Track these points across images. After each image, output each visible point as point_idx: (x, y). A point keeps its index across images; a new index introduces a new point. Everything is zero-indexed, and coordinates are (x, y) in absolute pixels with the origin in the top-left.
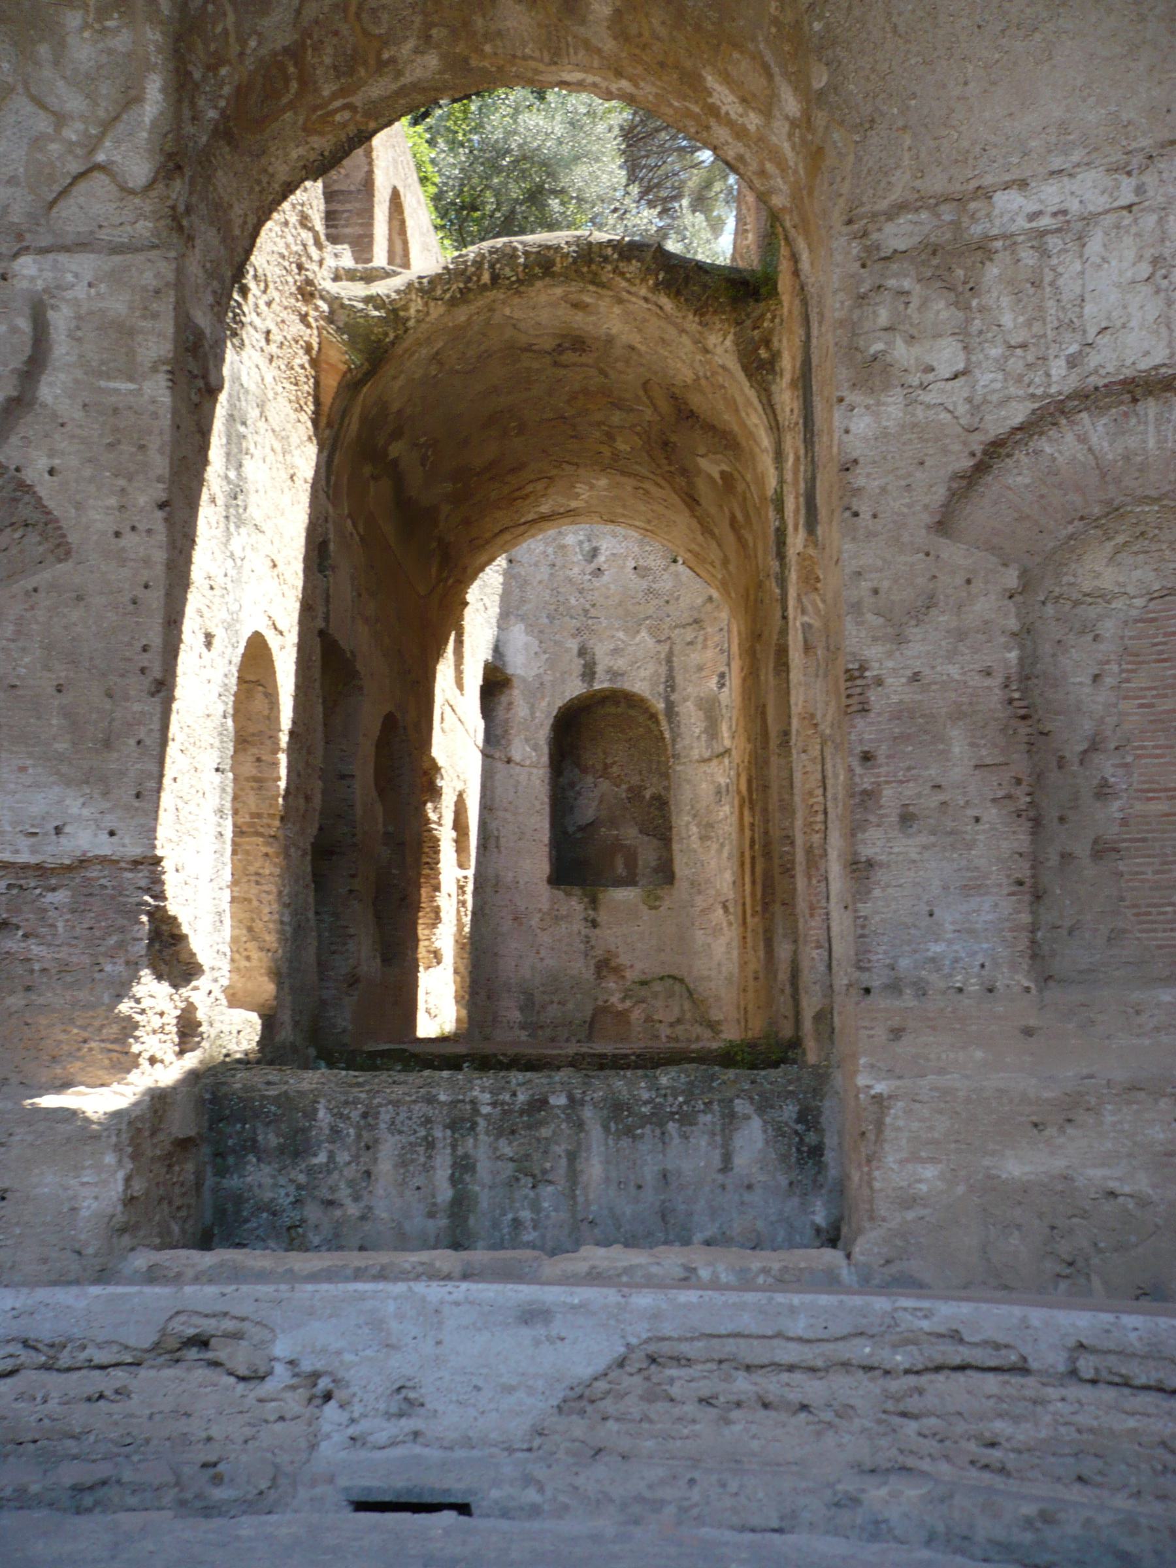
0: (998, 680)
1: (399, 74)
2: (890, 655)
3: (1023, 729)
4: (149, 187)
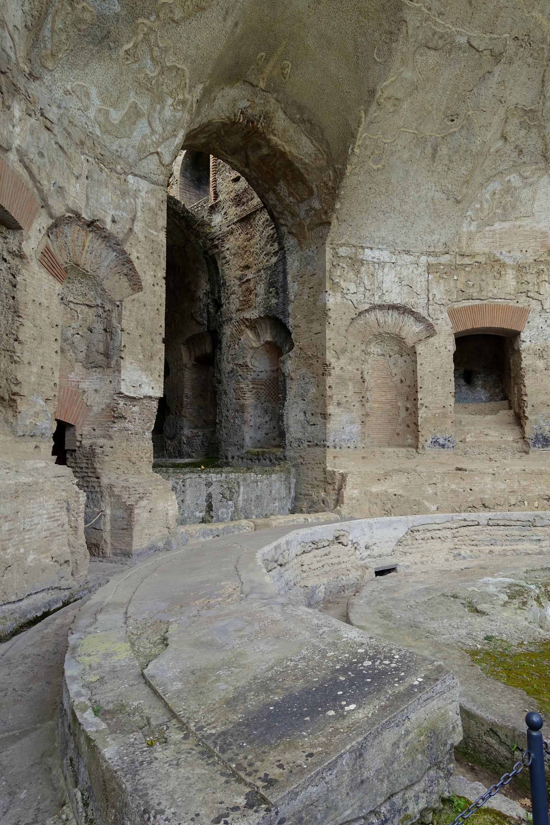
0: (360, 372)
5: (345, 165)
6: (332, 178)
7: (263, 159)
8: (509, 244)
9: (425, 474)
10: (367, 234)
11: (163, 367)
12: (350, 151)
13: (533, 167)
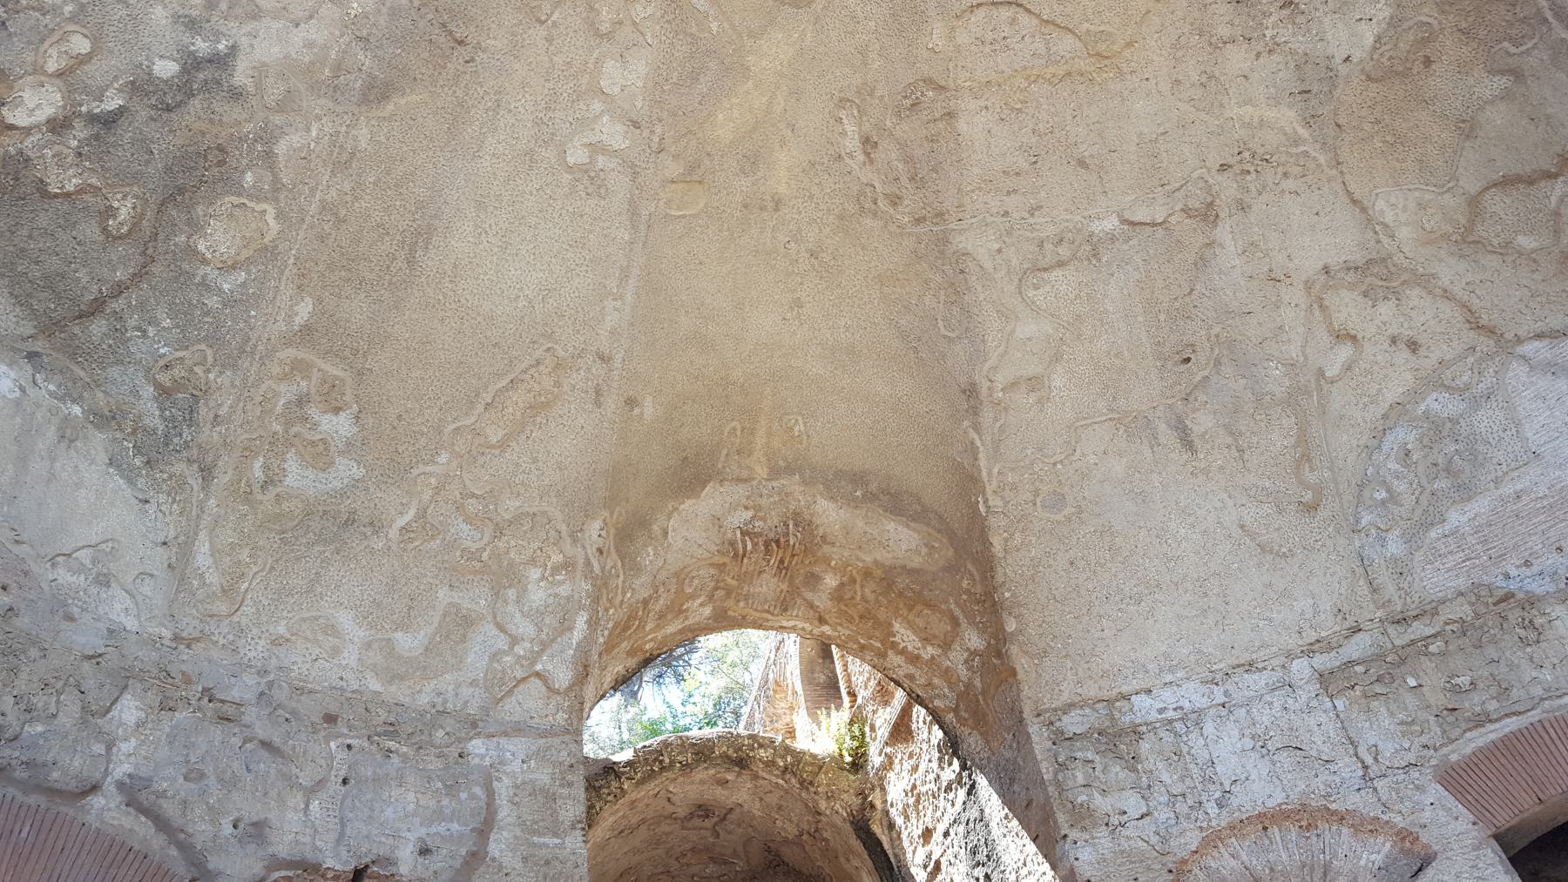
1: (687, 618)
4: (570, 688)
5: (987, 544)
6: (977, 577)
7: (838, 595)
8: (1516, 547)
12: (982, 509)
13: (1471, 360)
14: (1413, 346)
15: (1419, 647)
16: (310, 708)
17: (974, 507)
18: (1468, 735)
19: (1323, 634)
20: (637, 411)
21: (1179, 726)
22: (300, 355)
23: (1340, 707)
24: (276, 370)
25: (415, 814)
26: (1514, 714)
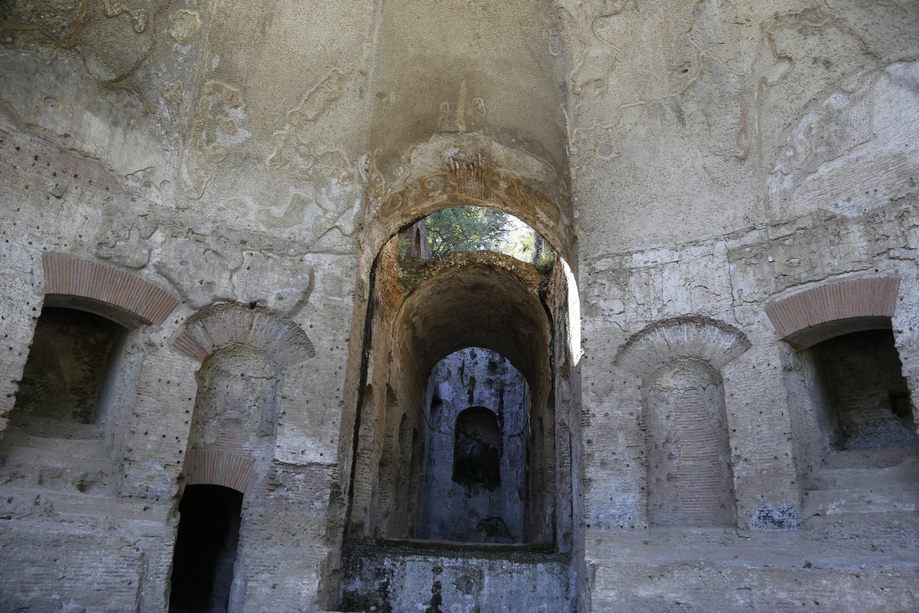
0: (635, 417)
2: (597, 406)
3: (644, 435)
4: (352, 234)
8: (847, 189)
9: (729, 571)
10: (630, 236)
11: (338, 432)
13: (860, 73)
14: (827, 64)
15: (781, 240)
16: (234, 238)
17: (564, 150)
18: (788, 289)
19: (736, 229)
20: (385, 99)
21: (652, 271)
22: (217, 82)
23: (732, 269)
24: (206, 91)
25: (277, 283)
26: (813, 281)
